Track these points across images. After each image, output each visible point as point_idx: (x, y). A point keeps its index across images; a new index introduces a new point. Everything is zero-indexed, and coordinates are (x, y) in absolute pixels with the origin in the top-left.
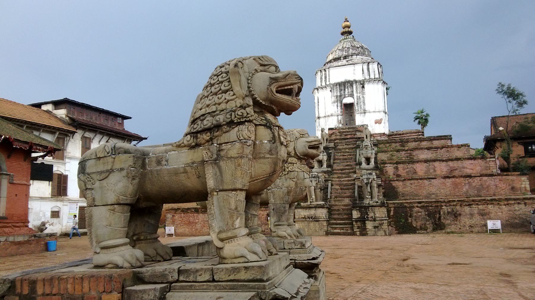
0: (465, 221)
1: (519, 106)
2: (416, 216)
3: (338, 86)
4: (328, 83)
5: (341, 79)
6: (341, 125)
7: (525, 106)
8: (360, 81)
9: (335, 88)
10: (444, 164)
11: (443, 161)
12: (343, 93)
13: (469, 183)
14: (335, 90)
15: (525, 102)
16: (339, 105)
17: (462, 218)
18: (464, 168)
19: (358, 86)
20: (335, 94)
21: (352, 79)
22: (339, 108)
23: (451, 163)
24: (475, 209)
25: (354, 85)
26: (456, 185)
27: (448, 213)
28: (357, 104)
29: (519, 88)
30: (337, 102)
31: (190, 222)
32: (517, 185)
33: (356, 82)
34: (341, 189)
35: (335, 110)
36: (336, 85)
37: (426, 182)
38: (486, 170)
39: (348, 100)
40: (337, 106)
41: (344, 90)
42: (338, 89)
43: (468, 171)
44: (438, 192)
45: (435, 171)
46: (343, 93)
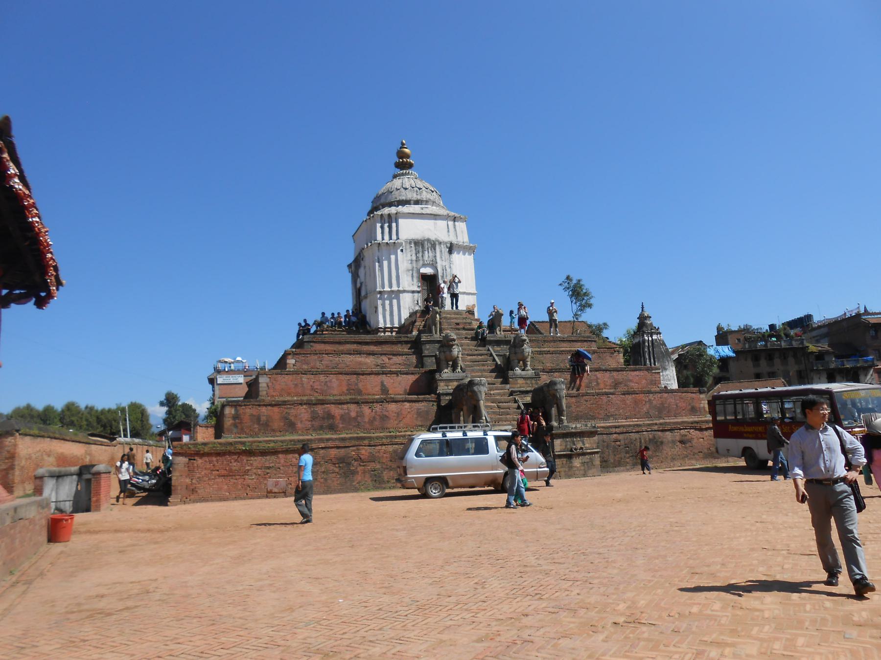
0: (667, 450)
1: (581, 310)
2: (614, 447)
3: (413, 245)
4: (394, 237)
5: (417, 235)
6: (417, 308)
7: (588, 310)
8: (446, 243)
9: (408, 246)
10: (607, 374)
11: (606, 370)
12: (421, 258)
13: (650, 400)
14: (409, 250)
15: (590, 306)
16: (415, 274)
17: (665, 448)
18: (631, 381)
19: (443, 250)
20: (409, 258)
21: (433, 238)
22: (415, 280)
23: (615, 374)
24: (677, 435)
25: (437, 247)
26: (636, 402)
27: (650, 440)
28: (443, 277)
29: (588, 285)
30: (412, 270)
31: (231, 470)
32: (697, 405)
33: (440, 243)
34: (499, 407)
35: (409, 282)
36: (410, 243)
37: (604, 398)
38: (652, 384)
39: (428, 271)
40: (412, 276)
41: (423, 252)
42: (413, 248)
43: (635, 386)
44: (617, 412)
45: (598, 384)
46: (421, 258)
